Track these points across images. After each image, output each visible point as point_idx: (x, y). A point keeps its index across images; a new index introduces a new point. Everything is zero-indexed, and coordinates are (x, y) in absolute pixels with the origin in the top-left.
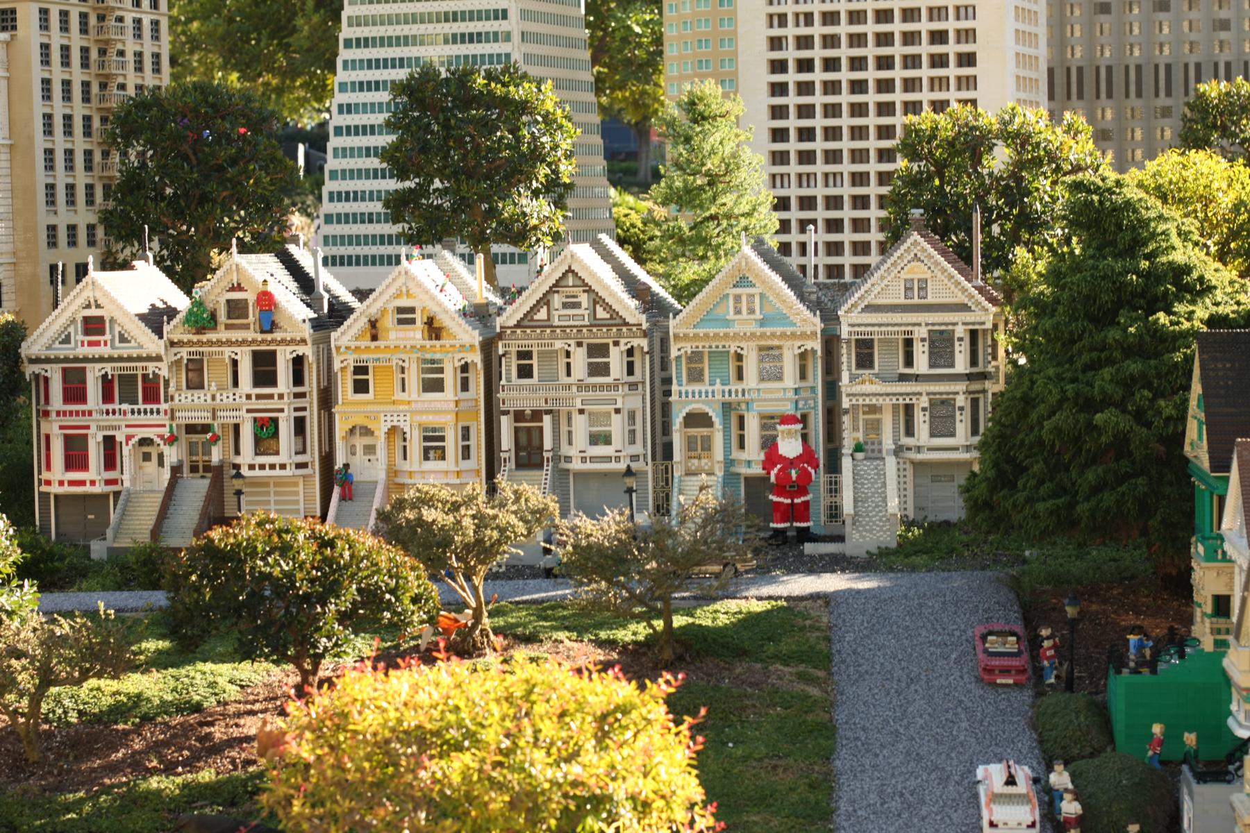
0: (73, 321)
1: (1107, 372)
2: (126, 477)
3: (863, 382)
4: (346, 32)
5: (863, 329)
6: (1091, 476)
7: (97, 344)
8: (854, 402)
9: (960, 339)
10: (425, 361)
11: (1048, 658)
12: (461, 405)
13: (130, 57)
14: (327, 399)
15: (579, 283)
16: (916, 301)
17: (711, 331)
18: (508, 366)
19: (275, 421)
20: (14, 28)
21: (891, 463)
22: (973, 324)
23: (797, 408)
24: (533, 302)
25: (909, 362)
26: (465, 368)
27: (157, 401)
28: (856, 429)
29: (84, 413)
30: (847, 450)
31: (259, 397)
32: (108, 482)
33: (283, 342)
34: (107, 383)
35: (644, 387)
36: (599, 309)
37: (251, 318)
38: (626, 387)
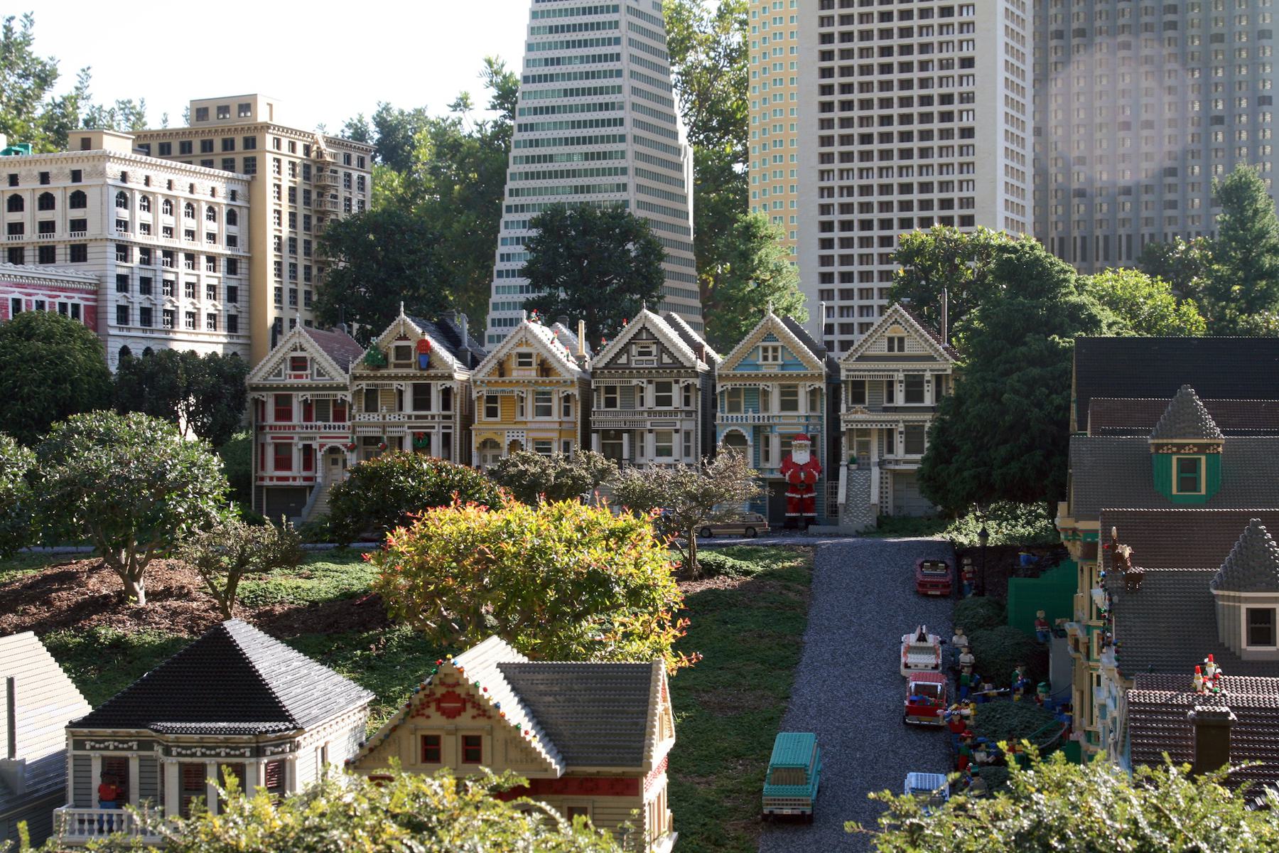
0: (284, 360)
1: (1015, 376)
2: (319, 474)
3: (856, 412)
4: (508, 201)
5: (857, 373)
6: (1003, 451)
7: (301, 377)
8: (849, 427)
9: (928, 382)
10: (538, 393)
11: (967, 579)
12: (564, 426)
13: (341, 200)
14: (468, 420)
15: (651, 337)
16: (896, 352)
17: (746, 372)
18: (599, 398)
19: (428, 435)
20: (254, 171)
21: (876, 472)
22: (938, 370)
23: (807, 431)
24: (616, 350)
25: (891, 399)
26: (567, 398)
27: (344, 420)
28: (851, 448)
29: (289, 427)
30: (844, 462)
31: (417, 417)
32: (306, 479)
33: (436, 377)
34: (307, 406)
35: (697, 415)
36: (665, 357)
37: (413, 360)
38: (684, 414)
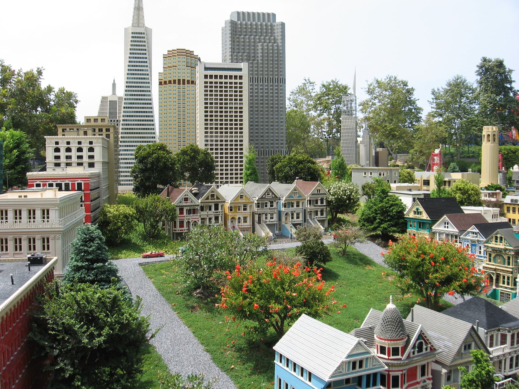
7: (187, 203)
19: (218, 217)
21: (316, 220)
25: (317, 203)
31: (216, 212)
